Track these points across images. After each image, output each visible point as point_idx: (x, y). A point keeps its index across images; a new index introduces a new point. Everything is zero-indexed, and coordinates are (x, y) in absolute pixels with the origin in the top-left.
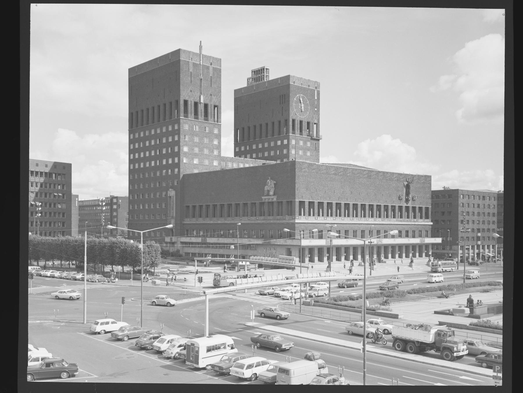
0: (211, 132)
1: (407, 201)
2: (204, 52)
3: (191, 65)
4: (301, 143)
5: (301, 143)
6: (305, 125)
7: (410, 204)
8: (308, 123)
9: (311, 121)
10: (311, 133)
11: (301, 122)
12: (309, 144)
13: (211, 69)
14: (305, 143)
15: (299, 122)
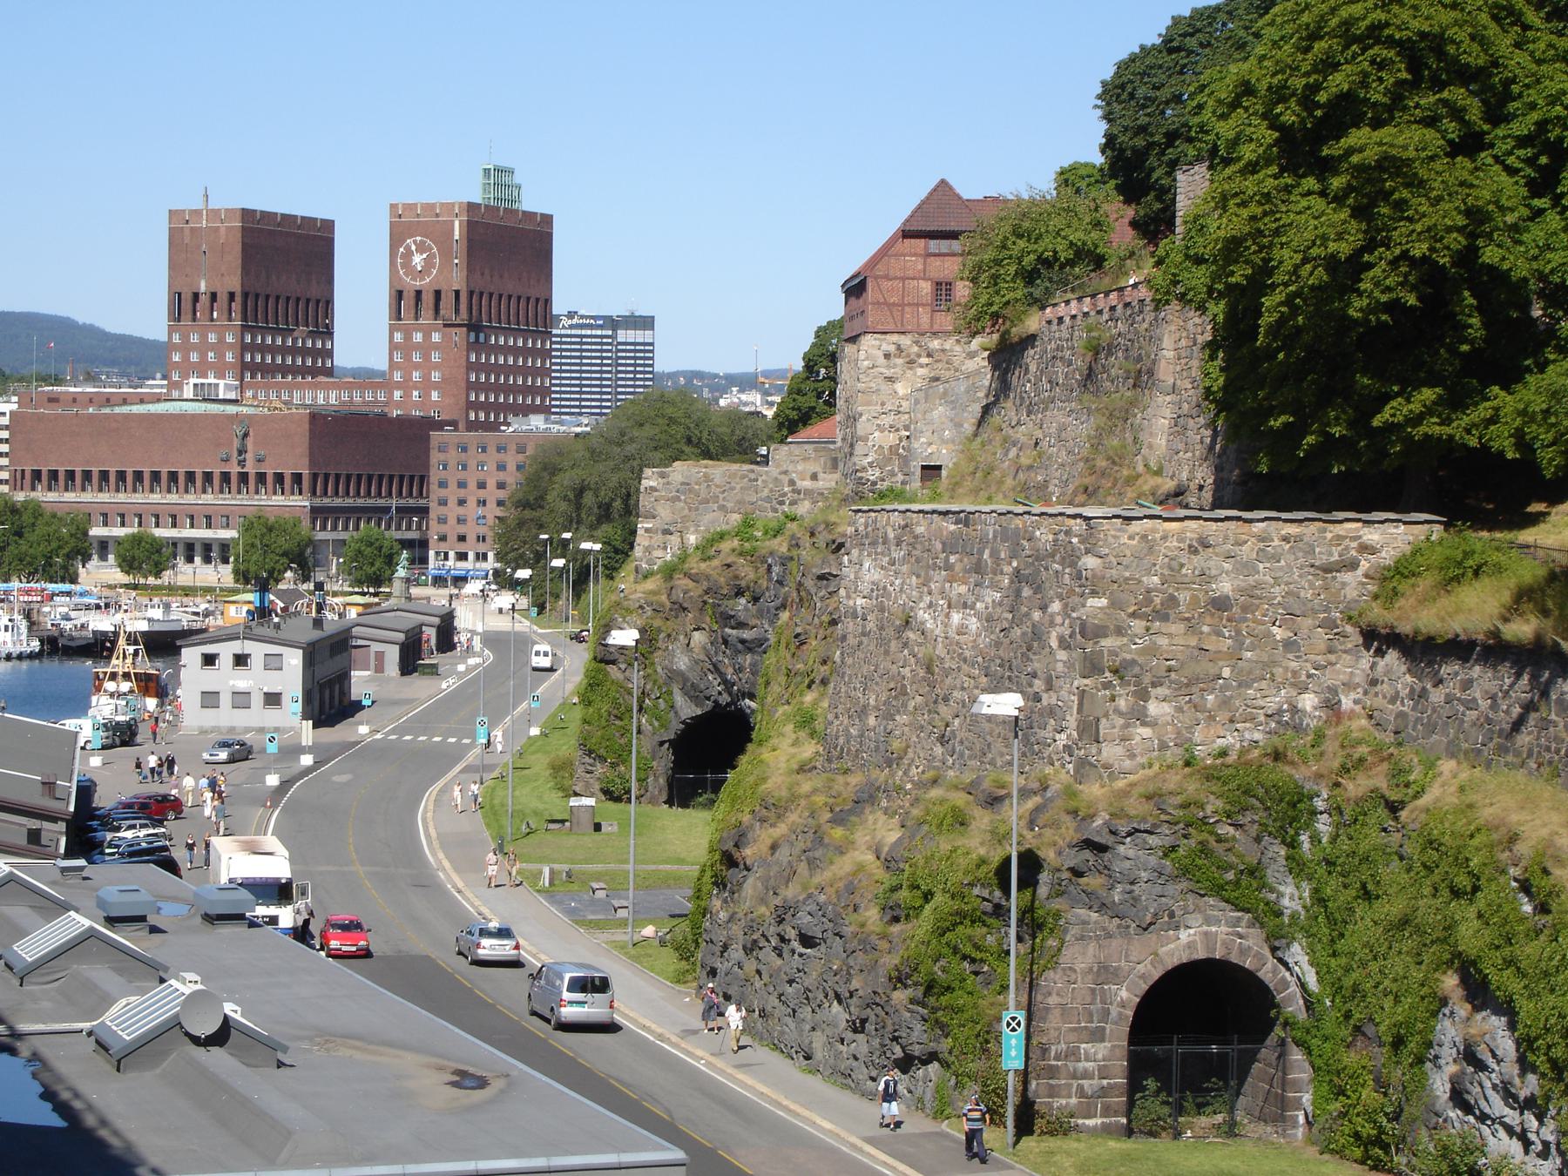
0: (221, 340)
1: (242, 463)
2: (214, 204)
3: (187, 232)
4: (418, 337)
5: (418, 337)
6: (428, 299)
7: (250, 468)
8: (438, 293)
9: (444, 287)
10: (442, 312)
11: (419, 293)
12: (436, 337)
13: (223, 231)
14: (427, 336)
15: (413, 294)
